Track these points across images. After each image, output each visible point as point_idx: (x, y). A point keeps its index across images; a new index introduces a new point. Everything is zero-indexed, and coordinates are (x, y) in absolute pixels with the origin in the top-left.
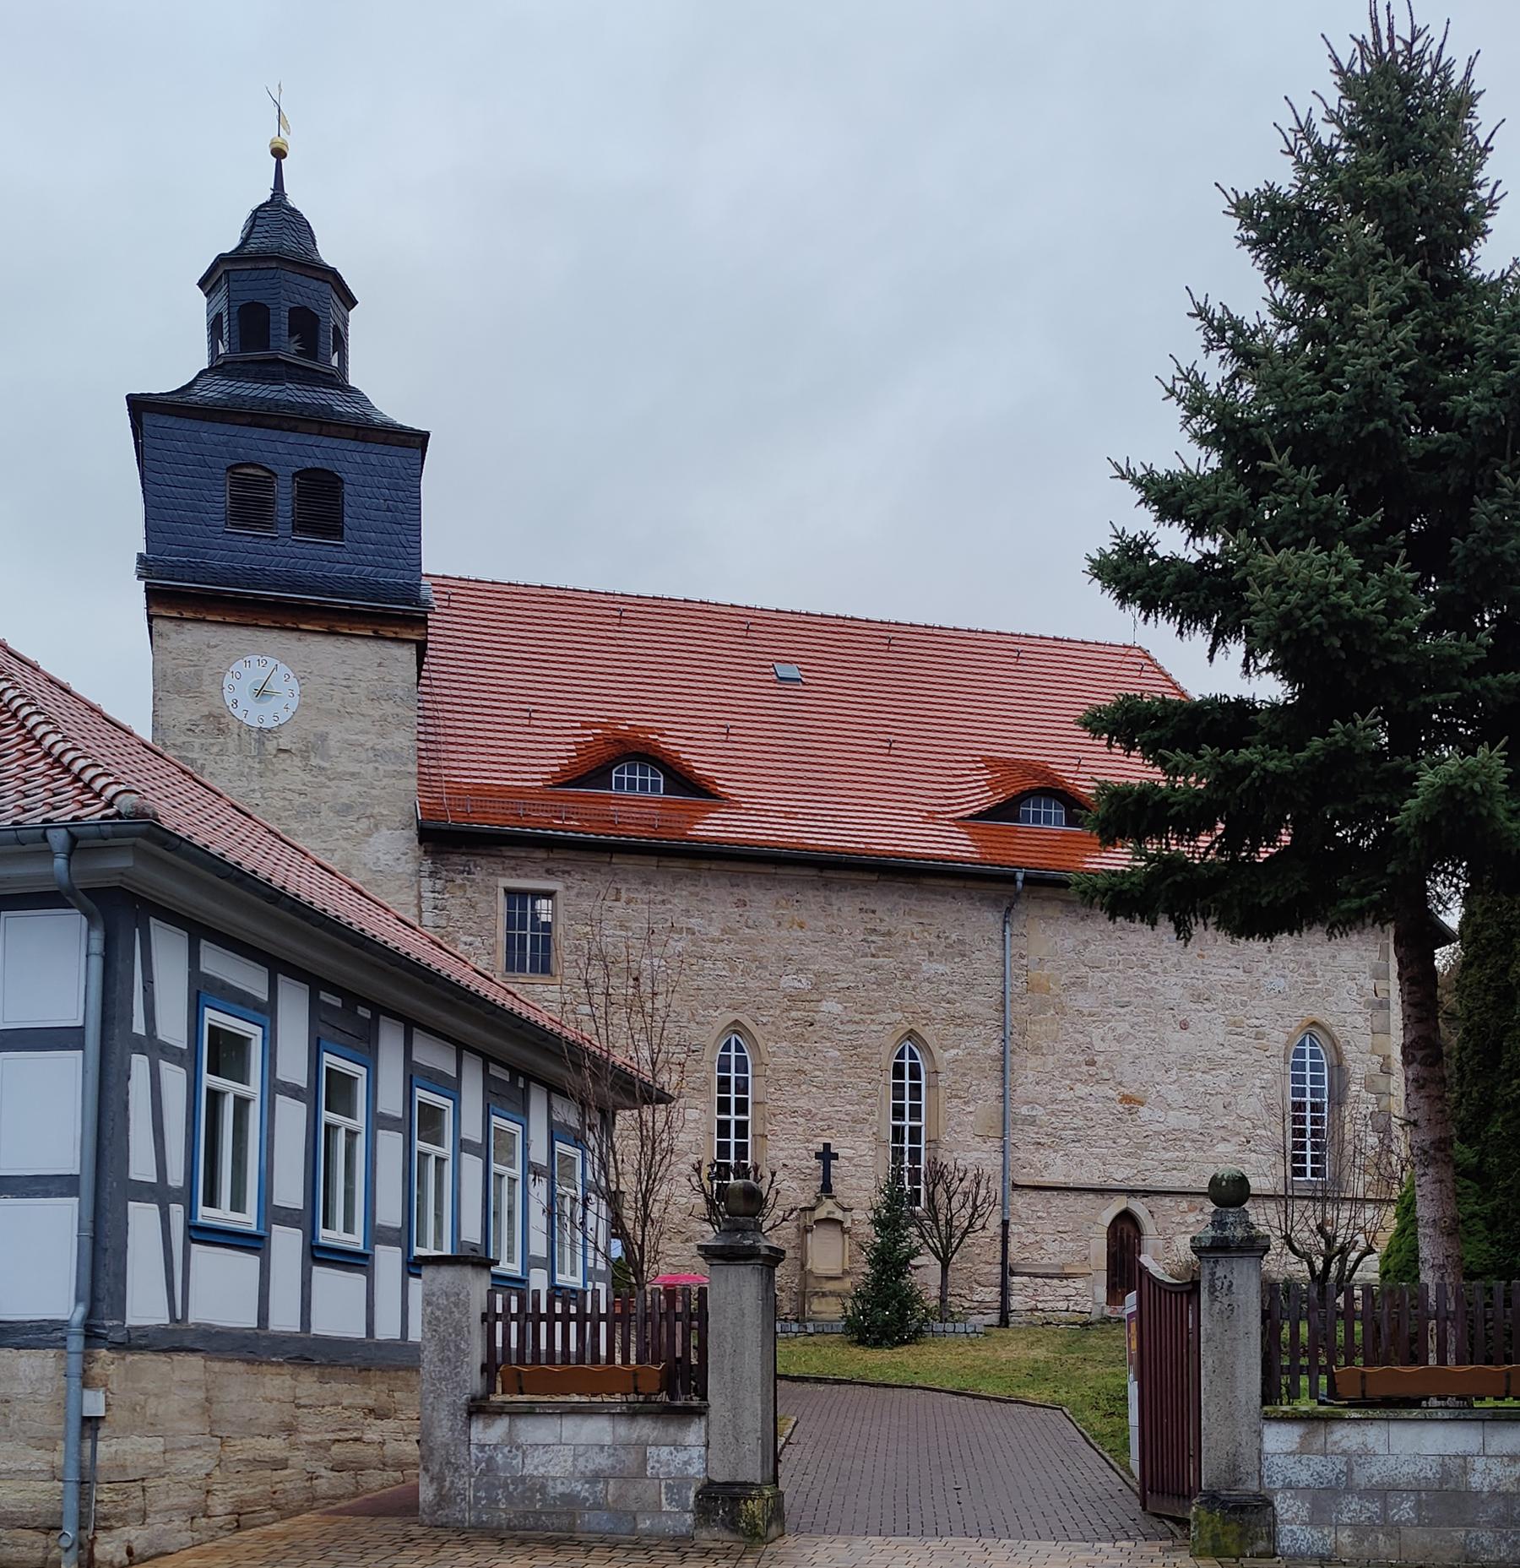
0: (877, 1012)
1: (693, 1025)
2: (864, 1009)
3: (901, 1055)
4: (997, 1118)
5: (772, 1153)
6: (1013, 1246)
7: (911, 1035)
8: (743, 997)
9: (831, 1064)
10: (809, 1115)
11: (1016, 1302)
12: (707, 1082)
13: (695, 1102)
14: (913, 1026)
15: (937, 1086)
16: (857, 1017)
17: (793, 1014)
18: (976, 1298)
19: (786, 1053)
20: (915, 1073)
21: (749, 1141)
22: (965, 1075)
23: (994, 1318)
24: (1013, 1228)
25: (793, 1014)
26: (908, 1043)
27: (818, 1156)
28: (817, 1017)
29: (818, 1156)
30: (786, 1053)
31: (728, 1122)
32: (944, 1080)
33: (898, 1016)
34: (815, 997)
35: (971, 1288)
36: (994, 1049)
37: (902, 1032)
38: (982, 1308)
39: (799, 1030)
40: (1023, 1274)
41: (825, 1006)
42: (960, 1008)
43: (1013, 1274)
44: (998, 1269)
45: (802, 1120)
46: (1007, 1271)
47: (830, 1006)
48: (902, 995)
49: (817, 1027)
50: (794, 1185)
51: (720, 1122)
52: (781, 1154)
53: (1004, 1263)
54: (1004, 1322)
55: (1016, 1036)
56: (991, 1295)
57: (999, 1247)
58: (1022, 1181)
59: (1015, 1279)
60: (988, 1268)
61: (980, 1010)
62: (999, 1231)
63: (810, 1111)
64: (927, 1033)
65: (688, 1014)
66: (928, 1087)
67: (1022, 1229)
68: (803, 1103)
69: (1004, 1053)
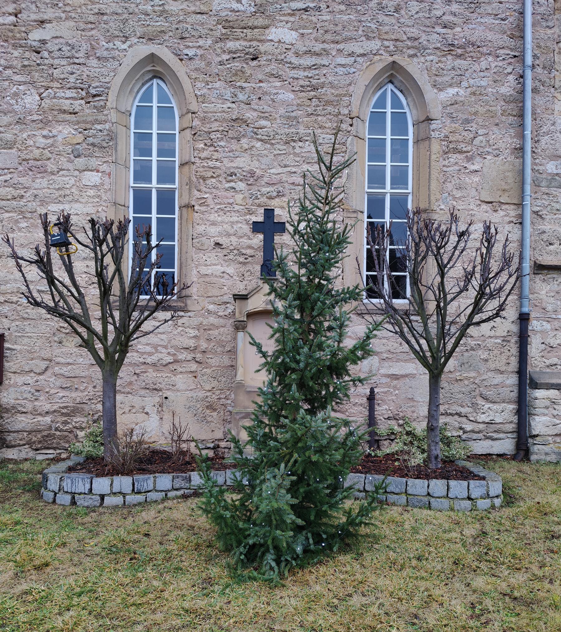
0: (347, 40)
1: (93, 62)
2: (328, 37)
3: (381, 103)
4: (511, 177)
5: (200, 229)
6: (534, 348)
7: (394, 74)
8: (161, 23)
9: (282, 111)
10: (251, 178)
11: (540, 424)
12: (112, 137)
13: (94, 162)
14: (396, 58)
15: (428, 138)
16: (318, 47)
17: (231, 45)
18: (482, 418)
19: (221, 97)
20: (399, 121)
21: (176, 216)
22: (467, 121)
23: (506, 445)
24: (534, 325)
25: (231, 45)
26: (390, 86)
27: (256, 227)
28: (262, 48)
29: (256, 227)
30: (221, 97)
31: (148, 192)
32: (439, 128)
33: (375, 45)
34: (260, 21)
35: (474, 405)
36: (508, 87)
37: (379, 66)
38: (491, 430)
39: (237, 65)
40: (549, 386)
41: (274, 33)
42: (459, 34)
43: (535, 385)
44: (513, 380)
45: (241, 185)
46: (526, 381)
47: (282, 33)
48: (381, 18)
49: (263, 60)
50: (230, 270)
51: (137, 192)
52: (213, 230)
53: (521, 371)
54: (522, 451)
55: (539, 70)
56: (504, 414)
57: (514, 350)
58: (548, 260)
59: (540, 393)
60: (499, 379)
61: (490, 36)
62: (515, 328)
63: (252, 174)
64: (414, 67)
65: (85, 47)
66: (417, 142)
67: (547, 326)
68: (243, 162)
69: (522, 92)
